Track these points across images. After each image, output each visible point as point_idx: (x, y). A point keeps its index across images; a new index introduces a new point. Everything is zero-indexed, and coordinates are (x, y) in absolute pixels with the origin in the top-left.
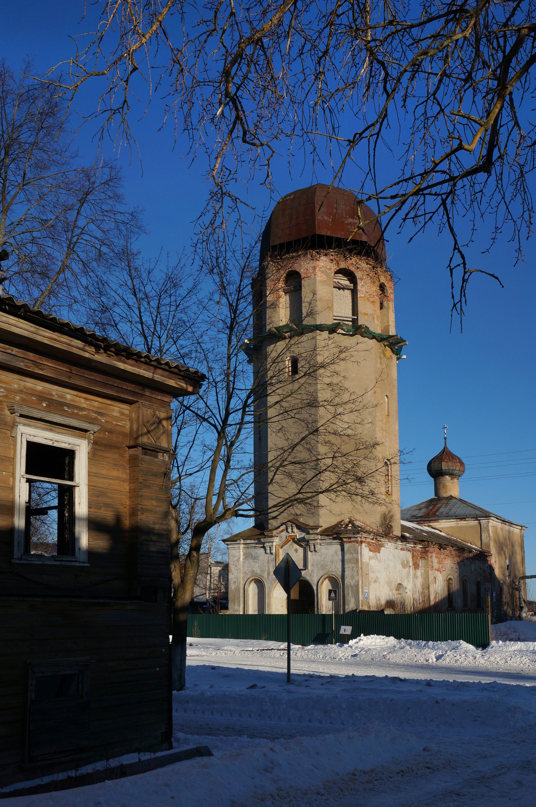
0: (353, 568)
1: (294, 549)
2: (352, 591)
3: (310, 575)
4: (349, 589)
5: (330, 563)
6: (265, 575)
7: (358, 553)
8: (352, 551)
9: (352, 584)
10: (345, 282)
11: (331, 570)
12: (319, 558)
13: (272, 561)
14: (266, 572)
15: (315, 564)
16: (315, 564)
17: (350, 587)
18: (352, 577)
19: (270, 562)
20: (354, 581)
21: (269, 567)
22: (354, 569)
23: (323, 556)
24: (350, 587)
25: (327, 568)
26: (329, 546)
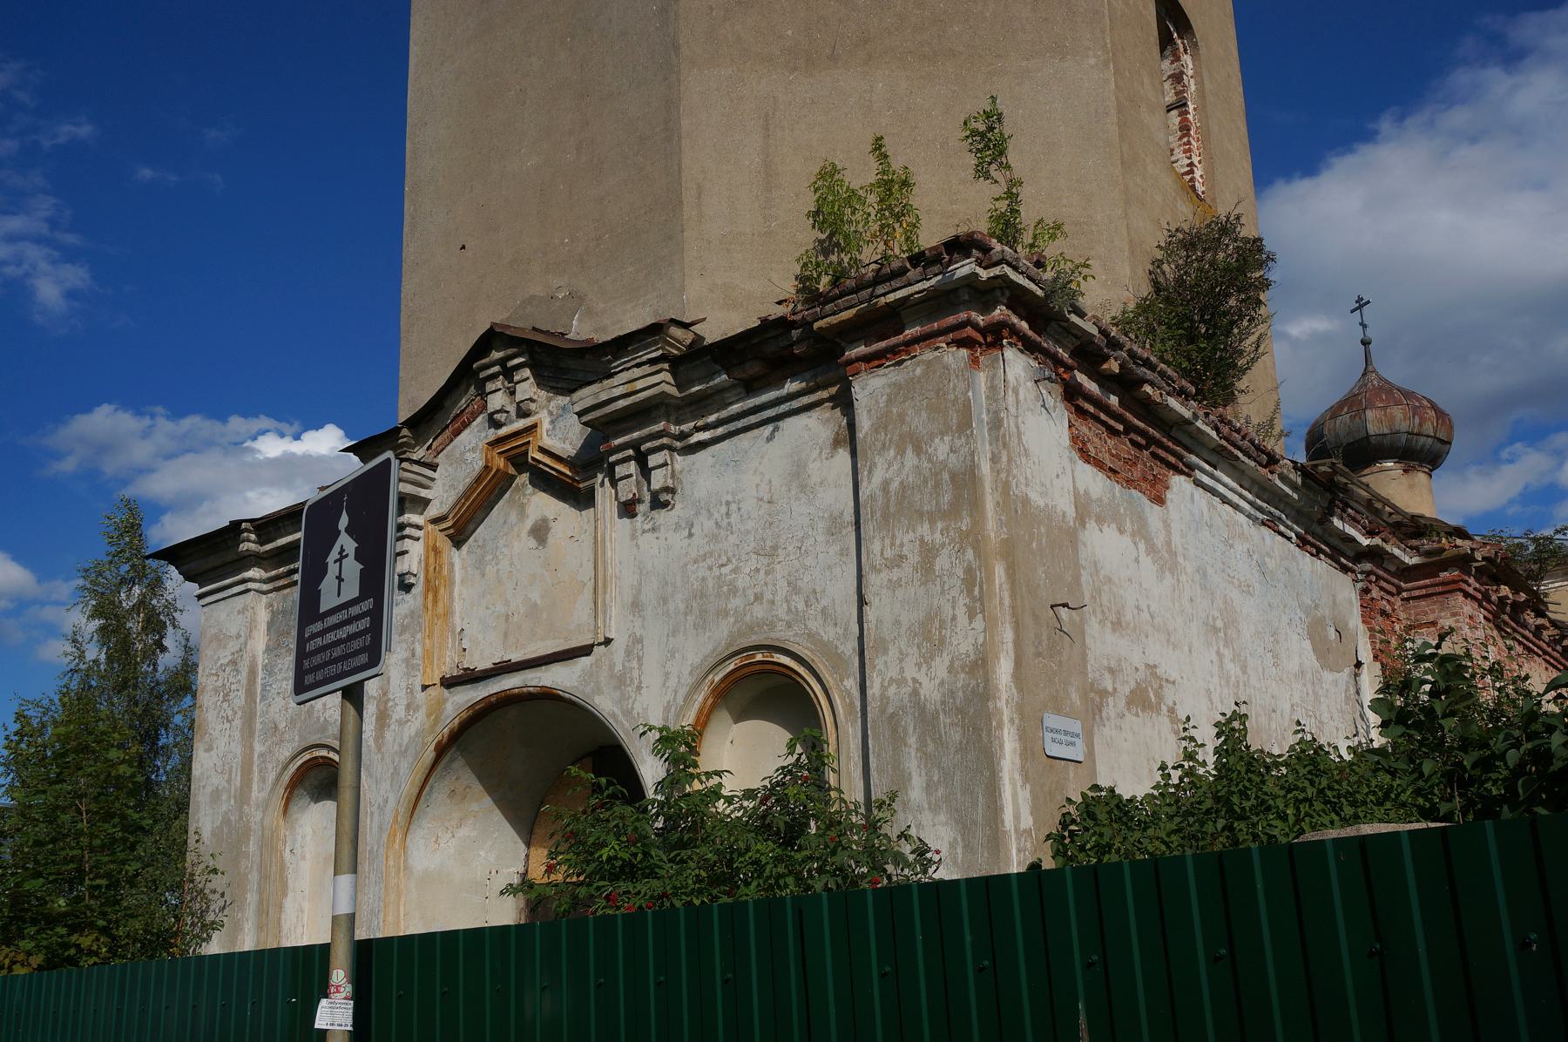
0: (929, 553)
1: (529, 524)
2: (926, 758)
3: (621, 681)
4: (898, 740)
5: (753, 562)
7: (965, 424)
8: (919, 421)
9: (930, 691)
11: (759, 611)
12: (678, 540)
17: (909, 722)
18: (930, 636)
20: (941, 666)
22: (942, 562)
23: (705, 525)
24: (909, 722)
25: (736, 602)
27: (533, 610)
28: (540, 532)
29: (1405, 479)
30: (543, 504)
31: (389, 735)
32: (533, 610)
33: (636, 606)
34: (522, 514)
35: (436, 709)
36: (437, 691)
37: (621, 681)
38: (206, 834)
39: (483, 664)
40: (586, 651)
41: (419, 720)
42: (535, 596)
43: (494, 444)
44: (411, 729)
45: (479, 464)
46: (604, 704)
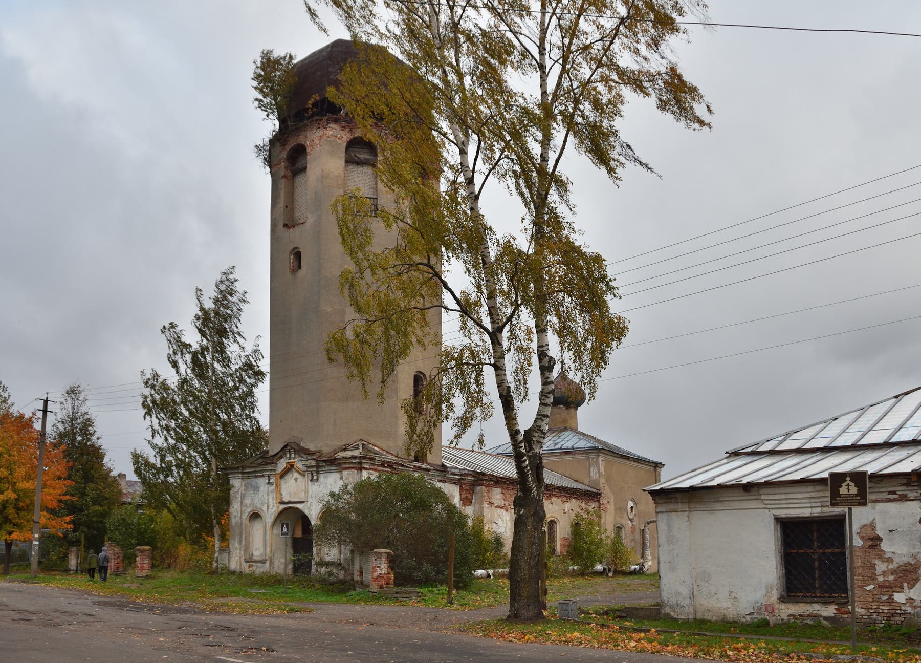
3: (309, 508)
6: (265, 508)
10: (363, 156)
13: (272, 492)
14: (266, 505)
15: (313, 495)
16: (313, 495)
19: (270, 493)
21: (268, 499)
26: (328, 474)
27: (295, 493)
28: (296, 480)
29: (566, 411)
30: (296, 475)
31: (269, 510)
32: (295, 493)
33: (311, 497)
34: (293, 476)
35: (278, 507)
36: (278, 504)
37: (309, 508)
38: (233, 523)
39: (286, 501)
40: (303, 502)
41: (275, 509)
42: (295, 490)
43: (287, 463)
44: (273, 510)
45: (285, 466)
46: (306, 512)
